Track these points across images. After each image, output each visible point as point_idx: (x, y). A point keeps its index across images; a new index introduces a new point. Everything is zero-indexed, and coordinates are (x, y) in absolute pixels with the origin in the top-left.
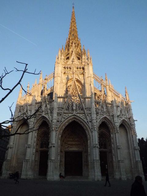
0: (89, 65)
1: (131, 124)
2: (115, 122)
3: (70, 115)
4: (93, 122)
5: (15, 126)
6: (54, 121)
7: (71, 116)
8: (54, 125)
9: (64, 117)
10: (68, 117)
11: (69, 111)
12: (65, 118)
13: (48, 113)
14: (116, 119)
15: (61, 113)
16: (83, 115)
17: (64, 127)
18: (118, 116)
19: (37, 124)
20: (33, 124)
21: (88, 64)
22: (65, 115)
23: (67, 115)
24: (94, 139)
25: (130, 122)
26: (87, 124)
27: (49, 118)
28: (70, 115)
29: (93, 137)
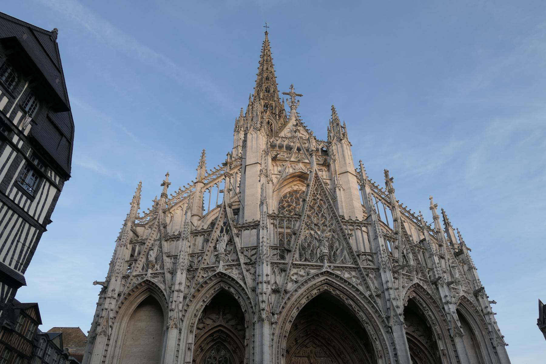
0: (343, 141)
1: (482, 310)
2: (444, 301)
3: (313, 271)
4: (387, 297)
5: (113, 307)
6: (265, 290)
7: (317, 275)
8: (263, 301)
9: (294, 278)
10: (309, 279)
11: (306, 260)
12: (296, 282)
13: (239, 265)
14: (444, 291)
15: (284, 264)
16: (353, 273)
17: (295, 313)
18: (449, 284)
19: (195, 301)
20: (181, 299)
21: (341, 140)
22: (294, 271)
23: (302, 272)
24: (399, 353)
25: (480, 305)
26: (369, 302)
27: (244, 279)
28: (313, 271)
29: (398, 347)
